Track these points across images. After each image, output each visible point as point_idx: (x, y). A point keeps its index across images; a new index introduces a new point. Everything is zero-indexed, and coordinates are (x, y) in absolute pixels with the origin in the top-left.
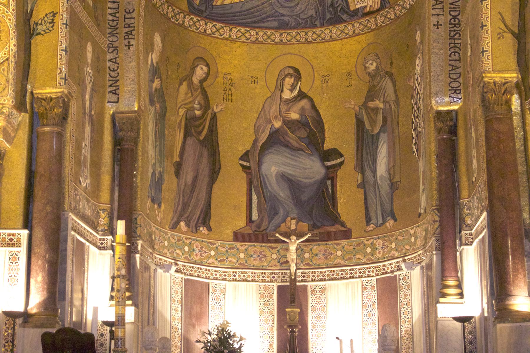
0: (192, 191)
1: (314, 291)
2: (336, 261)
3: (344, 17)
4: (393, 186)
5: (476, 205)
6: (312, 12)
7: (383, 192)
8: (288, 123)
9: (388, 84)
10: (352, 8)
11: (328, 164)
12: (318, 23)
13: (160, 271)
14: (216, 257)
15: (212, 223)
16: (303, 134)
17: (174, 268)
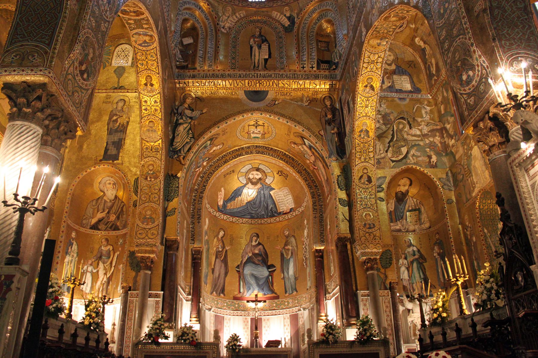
0: (218, 280)
1: (264, 320)
2: (274, 308)
3: (276, 215)
4: (296, 279)
5: (333, 284)
6: (263, 213)
7: (292, 281)
8: (254, 254)
9: (293, 240)
10: (279, 211)
11: (270, 270)
12: (265, 217)
13: (207, 311)
14: (227, 306)
15: (225, 293)
16: (260, 258)
17: (212, 310)
